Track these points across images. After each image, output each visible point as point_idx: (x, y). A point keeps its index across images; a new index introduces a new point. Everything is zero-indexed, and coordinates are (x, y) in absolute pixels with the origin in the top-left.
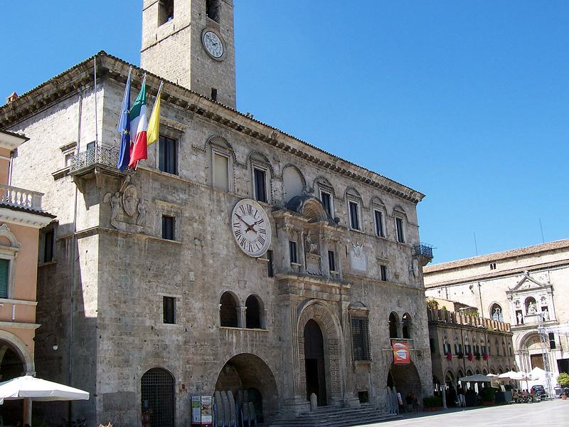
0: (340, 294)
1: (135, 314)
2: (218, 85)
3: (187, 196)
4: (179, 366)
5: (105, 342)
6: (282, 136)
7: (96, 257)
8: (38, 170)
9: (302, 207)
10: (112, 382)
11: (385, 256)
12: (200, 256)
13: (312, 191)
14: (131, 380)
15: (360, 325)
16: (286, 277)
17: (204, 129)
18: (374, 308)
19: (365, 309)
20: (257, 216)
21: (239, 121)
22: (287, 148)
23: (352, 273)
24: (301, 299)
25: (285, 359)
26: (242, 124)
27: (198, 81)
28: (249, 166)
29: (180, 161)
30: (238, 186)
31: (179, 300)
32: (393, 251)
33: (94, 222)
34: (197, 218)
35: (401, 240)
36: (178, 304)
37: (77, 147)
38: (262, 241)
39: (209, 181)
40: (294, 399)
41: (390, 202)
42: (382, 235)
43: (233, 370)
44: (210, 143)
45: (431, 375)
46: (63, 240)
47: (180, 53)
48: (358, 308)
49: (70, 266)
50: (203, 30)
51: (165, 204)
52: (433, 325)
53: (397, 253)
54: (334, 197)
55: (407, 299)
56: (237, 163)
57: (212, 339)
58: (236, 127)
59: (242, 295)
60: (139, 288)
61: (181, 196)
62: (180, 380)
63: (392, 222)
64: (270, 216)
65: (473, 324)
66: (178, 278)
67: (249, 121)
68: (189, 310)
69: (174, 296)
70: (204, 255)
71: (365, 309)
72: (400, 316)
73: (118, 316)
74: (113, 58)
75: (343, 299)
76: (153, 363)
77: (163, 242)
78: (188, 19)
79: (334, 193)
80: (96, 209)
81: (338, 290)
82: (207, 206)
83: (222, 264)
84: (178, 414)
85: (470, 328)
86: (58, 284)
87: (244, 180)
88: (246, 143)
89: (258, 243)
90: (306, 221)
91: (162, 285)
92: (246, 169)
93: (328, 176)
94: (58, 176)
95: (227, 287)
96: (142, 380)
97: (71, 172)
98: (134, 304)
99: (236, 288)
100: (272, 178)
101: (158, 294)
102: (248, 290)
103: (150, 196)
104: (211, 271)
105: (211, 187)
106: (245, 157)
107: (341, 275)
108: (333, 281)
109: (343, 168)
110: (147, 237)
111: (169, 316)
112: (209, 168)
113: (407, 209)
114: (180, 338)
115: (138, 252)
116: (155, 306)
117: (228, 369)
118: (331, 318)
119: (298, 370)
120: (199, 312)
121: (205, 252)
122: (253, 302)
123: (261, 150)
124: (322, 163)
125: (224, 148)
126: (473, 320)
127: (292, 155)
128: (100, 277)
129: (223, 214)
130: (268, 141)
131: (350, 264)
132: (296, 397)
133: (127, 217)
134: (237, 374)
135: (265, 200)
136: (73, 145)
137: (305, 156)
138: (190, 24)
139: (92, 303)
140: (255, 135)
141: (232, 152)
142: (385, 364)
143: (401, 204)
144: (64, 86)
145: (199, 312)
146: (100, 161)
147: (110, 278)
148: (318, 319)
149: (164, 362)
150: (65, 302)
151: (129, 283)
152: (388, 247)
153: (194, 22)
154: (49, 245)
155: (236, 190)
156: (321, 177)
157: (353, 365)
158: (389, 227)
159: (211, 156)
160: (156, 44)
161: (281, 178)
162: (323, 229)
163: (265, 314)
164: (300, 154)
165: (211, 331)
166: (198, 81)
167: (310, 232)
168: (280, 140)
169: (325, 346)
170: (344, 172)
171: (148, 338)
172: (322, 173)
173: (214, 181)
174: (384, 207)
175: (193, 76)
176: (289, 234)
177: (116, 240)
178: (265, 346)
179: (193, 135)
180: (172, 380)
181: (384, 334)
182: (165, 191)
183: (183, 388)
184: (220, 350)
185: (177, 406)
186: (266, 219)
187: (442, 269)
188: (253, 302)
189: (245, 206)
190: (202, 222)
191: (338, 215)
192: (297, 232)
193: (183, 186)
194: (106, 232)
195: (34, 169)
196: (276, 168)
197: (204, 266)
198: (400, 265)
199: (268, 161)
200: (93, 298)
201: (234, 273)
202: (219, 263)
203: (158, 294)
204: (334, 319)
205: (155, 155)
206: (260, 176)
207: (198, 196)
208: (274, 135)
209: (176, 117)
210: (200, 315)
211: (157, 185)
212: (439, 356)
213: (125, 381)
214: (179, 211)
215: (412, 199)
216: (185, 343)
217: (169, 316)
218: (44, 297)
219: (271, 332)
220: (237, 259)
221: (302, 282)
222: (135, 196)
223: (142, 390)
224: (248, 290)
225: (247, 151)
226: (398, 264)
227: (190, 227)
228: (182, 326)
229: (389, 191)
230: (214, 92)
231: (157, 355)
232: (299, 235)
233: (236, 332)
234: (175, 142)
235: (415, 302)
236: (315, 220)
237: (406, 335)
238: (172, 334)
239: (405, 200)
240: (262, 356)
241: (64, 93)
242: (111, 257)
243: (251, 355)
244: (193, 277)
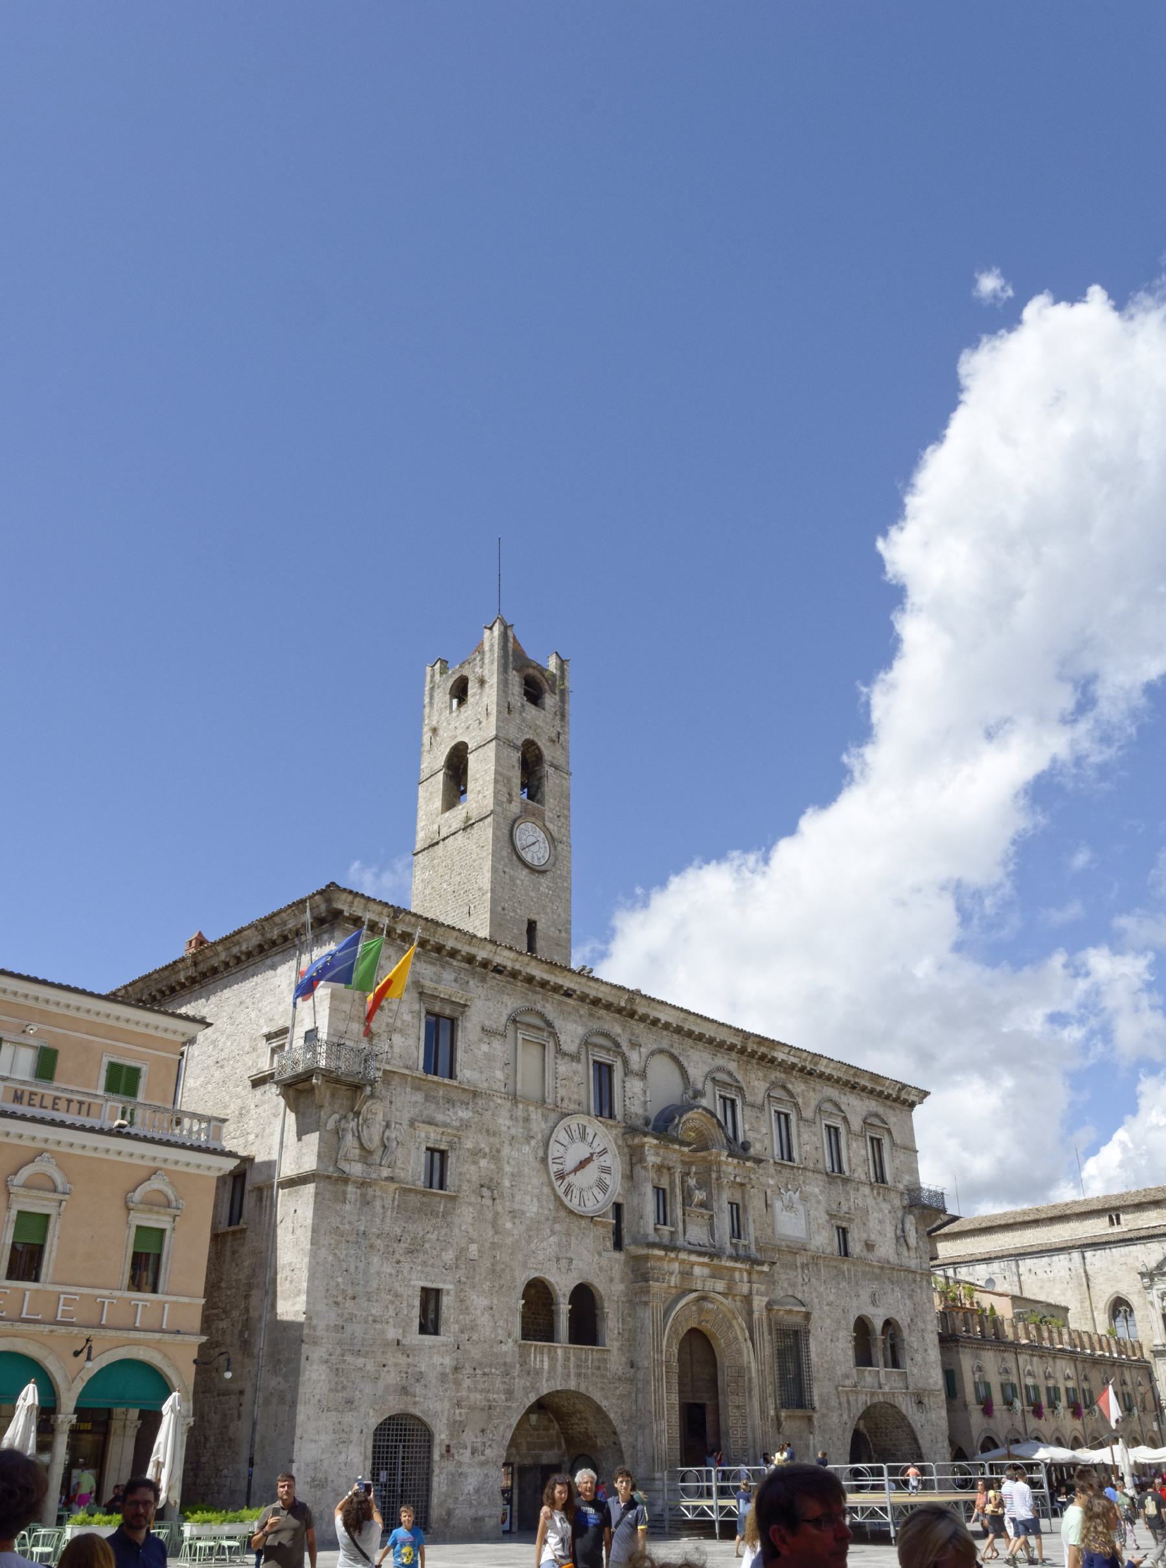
0: (750, 1282)
1: (370, 1318)
2: (538, 913)
3: (470, 1114)
4: (442, 1412)
5: (315, 1367)
6: (644, 1001)
7: (309, 1222)
8: (227, 1069)
9: (677, 1125)
10: (323, 1437)
11: (844, 1208)
12: (489, 1216)
13: (698, 1094)
14: (355, 1436)
15: (791, 1344)
16: (644, 1251)
17: (506, 998)
18: (821, 1309)
19: (803, 1309)
20: (595, 1144)
21: (567, 982)
22: (655, 1022)
23: (779, 1243)
24: (674, 1291)
25: (640, 1401)
26: (572, 986)
27: (504, 909)
28: (583, 1057)
29: (460, 1055)
30: (562, 1092)
31: (448, 1293)
32: (864, 1197)
33: (310, 1163)
34: (487, 1150)
35: (881, 1178)
36: (446, 1301)
37: (289, 1035)
38: (602, 1186)
39: (510, 1087)
40: (654, 1479)
41: (857, 1107)
42: (841, 1170)
43: (550, 1421)
44: (514, 1021)
45: (946, 1443)
46: (260, 1190)
47: (474, 861)
48: (788, 1308)
49: (268, 1235)
50: (515, 821)
51: (431, 1129)
52: (948, 1341)
53: (870, 1201)
54: (744, 1103)
56: (559, 1051)
57: (505, 1364)
58: (562, 992)
59: (563, 1285)
60: (378, 1273)
61: (460, 1113)
62: (443, 1436)
63: (862, 1144)
64: (620, 1142)
65: (1046, 1344)
66: (449, 1256)
67: (584, 980)
68: (466, 1311)
69: (440, 1286)
70: (497, 1214)
71: (803, 1309)
72: (878, 1324)
73: (340, 1322)
74: (351, 892)
75: (754, 1292)
76: (395, 1405)
77: (425, 1194)
78: (489, 803)
79: (743, 1097)
80: (313, 1138)
81: (745, 1274)
82: (504, 1129)
83: (529, 1229)
84: (435, 1500)
85: (1035, 1349)
86: (246, 1264)
87: (574, 1082)
88: (581, 1016)
89: (596, 1191)
90: (686, 1149)
91: (419, 1268)
92: (579, 1061)
93: (732, 1066)
94: (257, 1083)
95: (536, 1269)
96: (375, 1435)
97: (276, 1078)
98: (369, 1300)
99: (553, 1271)
100: (626, 1075)
101: (412, 1283)
102: (574, 1274)
103: (406, 1116)
104: (509, 1240)
105: (514, 1098)
106: (577, 1041)
107: (753, 1247)
108: (736, 1258)
109: (763, 1050)
110: (397, 1186)
111: (430, 1324)
112: (511, 1065)
113: (893, 1119)
114: (447, 1361)
115: (381, 1211)
116: (405, 1304)
117: (534, 1418)
118: (731, 1326)
119: (664, 1425)
120: (483, 1314)
121: (499, 1209)
122: (585, 1299)
123: (606, 1027)
124: (721, 1044)
125: (539, 1029)
126: (1046, 1335)
127: (665, 1033)
128: (313, 1255)
129: (533, 1142)
130: (619, 1011)
131: (772, 1225)
132: (658, 1475)
133: (364, 1153)
134: (557, 1426)
135: (611, 1116)
136: (284, 1032)
137: (690, 1034)
138: (492, 812)
139: (298, 1299)
140: (596, 1002)
141: (554, 1035)
142: (845, 1417)
143: (881, 1110)
144: (275, 934)
145: (483, 1314)
146: (323, 1063)
147: (330, 1258)
148: (706, 1327)
149: (415, 1403)
150: (256, 1295)
151: (361, 1266)
152: (852, 1192)
153: (499, 809)
154: (238, 1196)
155: (559, 1099)
156: (720, 1069)
157: (778, 1417)
158: (856, 1154)
159: (516, 1044)
160: (437, 843)
161: (643, 1075)
162: (719, 1163)
163: (603, 1319)
164: (679, 1030)
165: (504, 1348)
166: (504, 909)
167: (694, 1169)
168: (641, 1010)
169: (724, 1378)
170: (763, 1057)
171: (391, 1361)
172: (721, 1061)
173: (519, 1087)
174: (845, 1119)
175: (494, 901)
176: (652, 1174)
177: (344, 1193)
178: (603, 1376)
179: (486, 1007)
180: (428, 1436)
181: (841, 1358)
182: (433, 1106)
183: (448, 1451)
184: (519, 1383)
185: (435, 1485)
186: (612, 1148)
187: (1012, 1221)
188: (584, 1297)
189: (574, 1127)
190: (495, 1156)
191: (751, 1136)
192: (669, 1169)
193: (465, 1097)
194: (329, 1180)
195: (222, 1067)
196: (635, 1058)
197: (496, 1233)
198: (878, 1224)
199: (618, 1045)
200: (299, 1291)
201: (549, 1245)
202: (523, 1228)
203: (412, 1283)
204: (737, 1327)
205: (418, 1048)
206: (603, 1072)
207: (490, 1112)
208: (631, 1000)
209: (455, 981)
210: (484, 1320)
211: (419, 1097)
212: (965, 1406)
213: (344, 1436)
214: (456, 1140)
215: (904, 1099)
216: (456, 1369)
217: (430, 1324)
218: (223, 1285)
219: (615, 1352)
221: (671, 1260)
222: (380, 1116)
223: (374, 1452)
224: (574, 1274)
225: (581, 1031)
226: (873, 1224)
227: (473, 1168)
228: (452, 1339)
229: (853, 1088)
230: (532, 926)
231: (404, 1391)
232: (671, 1175)
233: (550, 1351)
234: (453, 1021)
235: (911, 1297)
236: (706, 1148)
237: (896, 1364)
238: (434, 1355)
239: (888, 1103)
240: (597, 1396)
241: (273, 943)
242: (335, 1221)
243: (577, 1394)
244: (476, 1253)
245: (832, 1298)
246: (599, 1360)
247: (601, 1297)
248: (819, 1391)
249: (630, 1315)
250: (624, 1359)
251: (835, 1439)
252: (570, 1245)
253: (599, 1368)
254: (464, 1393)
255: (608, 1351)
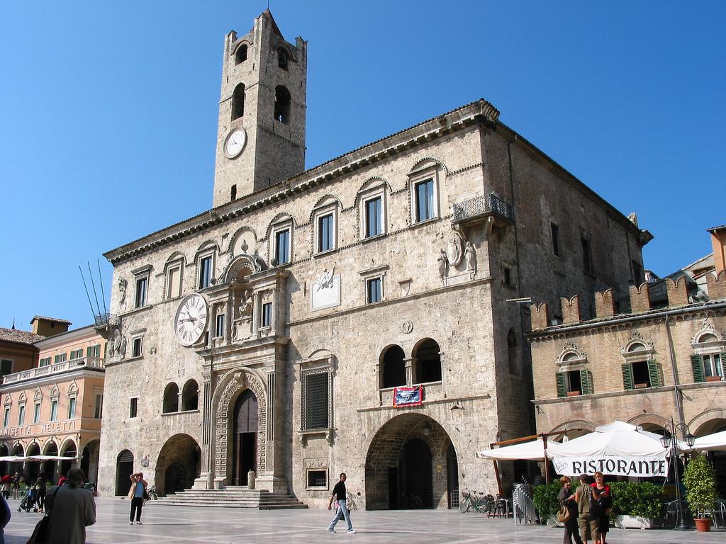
6: (220, 211)
55: (430, 313)
59: (181, 383)
114: (138, 427)
122: (192, 386)
142: (364, 430)
216: (141, 430)
231: (126, 441)
245: (359, 340)
248: (338, 416)
251: (353, 448)
253: (194, 421)
254: (143, 440)
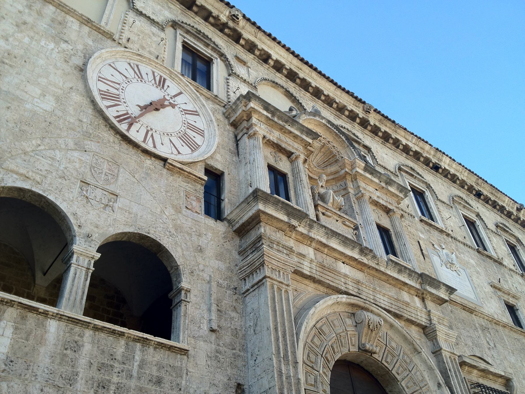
100: (229, 75)
168: (248, 33)
208: (234, 18)
219: (202, 360)
220: (87, 135)
224: (118, 215)
246: (160, 366)
247: (177, 268)
249: (235, 309)
250: (221, 378)
252: (116, 177)
255: (184, 352)
